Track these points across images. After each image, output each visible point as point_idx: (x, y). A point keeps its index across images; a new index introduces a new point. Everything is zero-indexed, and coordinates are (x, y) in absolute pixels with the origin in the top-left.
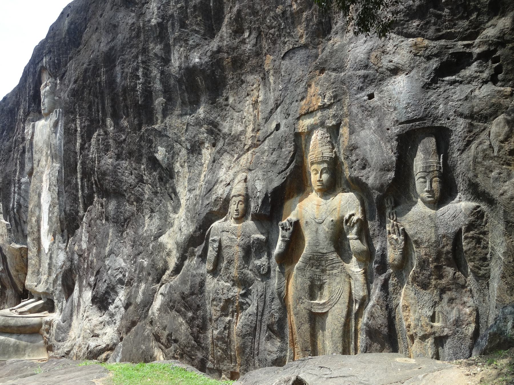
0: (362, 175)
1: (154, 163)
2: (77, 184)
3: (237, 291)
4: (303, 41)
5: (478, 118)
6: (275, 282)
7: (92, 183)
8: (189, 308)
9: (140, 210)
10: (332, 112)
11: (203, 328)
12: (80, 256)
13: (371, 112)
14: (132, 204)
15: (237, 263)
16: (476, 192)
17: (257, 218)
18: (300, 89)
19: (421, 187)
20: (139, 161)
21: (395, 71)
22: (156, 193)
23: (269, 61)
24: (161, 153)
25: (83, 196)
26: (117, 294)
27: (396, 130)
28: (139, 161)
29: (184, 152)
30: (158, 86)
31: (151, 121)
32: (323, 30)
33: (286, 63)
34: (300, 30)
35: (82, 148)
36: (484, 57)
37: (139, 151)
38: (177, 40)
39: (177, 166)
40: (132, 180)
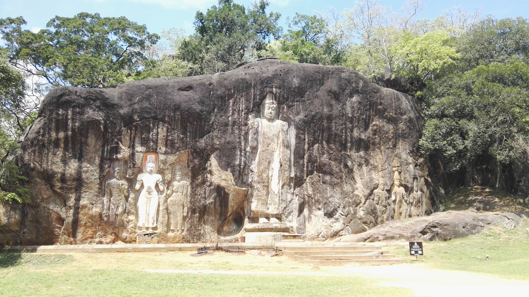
0: (407, 184)
1: (346, 166)
2: (304, 164)
3: (384, 208)
4: (391, 146)
5: (421, 177)
6: (393, 206)
7: (314, 166)
8: (373, 213)
9: (342, 182)
10: (400, 168)
11: (377, 219)
12: (309, 197)
13: (408, 171)
14: (338, 179)
15: (384, 202)
16: (422, 190)
17: (387, 190)
18: (392, 159)
19: (415, 188)
20: (340, 163)
21: (410, 163)
22: (346, 177)
23: (382, 148)
24: (349, 164)
25: (307, 170)
26: (337, 211)
27: (412, 177)
28: (340, 163)
29: (356, 165)
30: (349, 139)
31: (345, 150)
32: (395, 146)
33: (387, 150)
34: (390, 143)
35: (309, 149)
36: (419, 165)
37: (342, 160)
38: (356, 126)
39: (355, 170)
40: (337, 170)
